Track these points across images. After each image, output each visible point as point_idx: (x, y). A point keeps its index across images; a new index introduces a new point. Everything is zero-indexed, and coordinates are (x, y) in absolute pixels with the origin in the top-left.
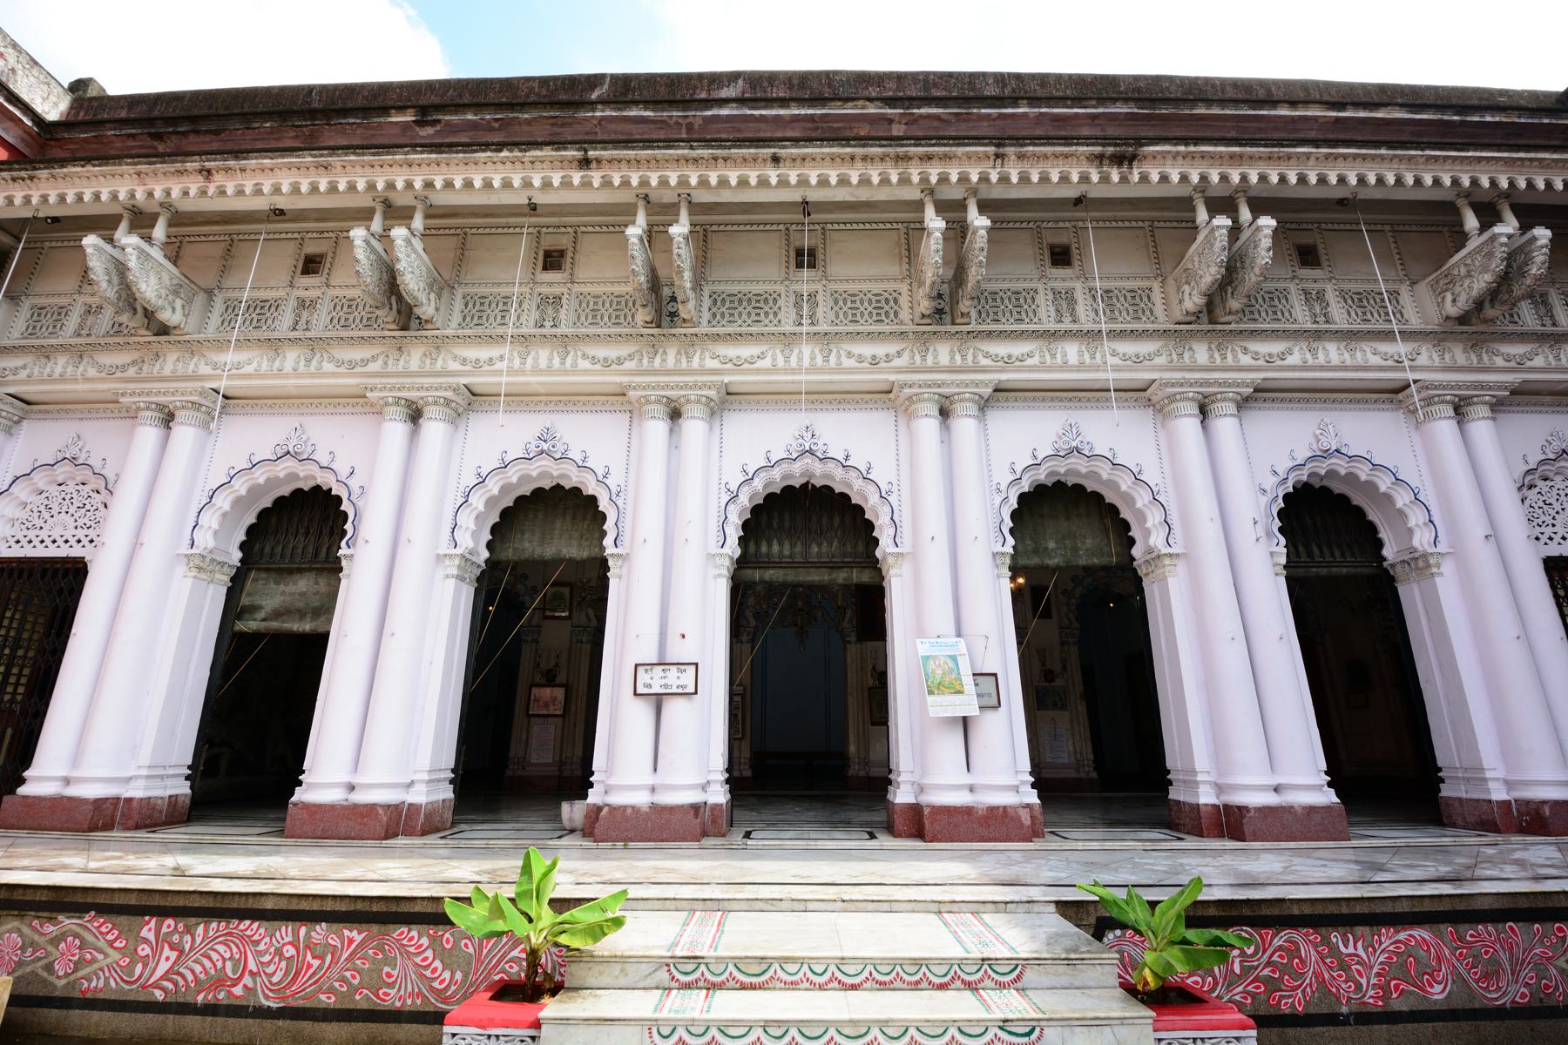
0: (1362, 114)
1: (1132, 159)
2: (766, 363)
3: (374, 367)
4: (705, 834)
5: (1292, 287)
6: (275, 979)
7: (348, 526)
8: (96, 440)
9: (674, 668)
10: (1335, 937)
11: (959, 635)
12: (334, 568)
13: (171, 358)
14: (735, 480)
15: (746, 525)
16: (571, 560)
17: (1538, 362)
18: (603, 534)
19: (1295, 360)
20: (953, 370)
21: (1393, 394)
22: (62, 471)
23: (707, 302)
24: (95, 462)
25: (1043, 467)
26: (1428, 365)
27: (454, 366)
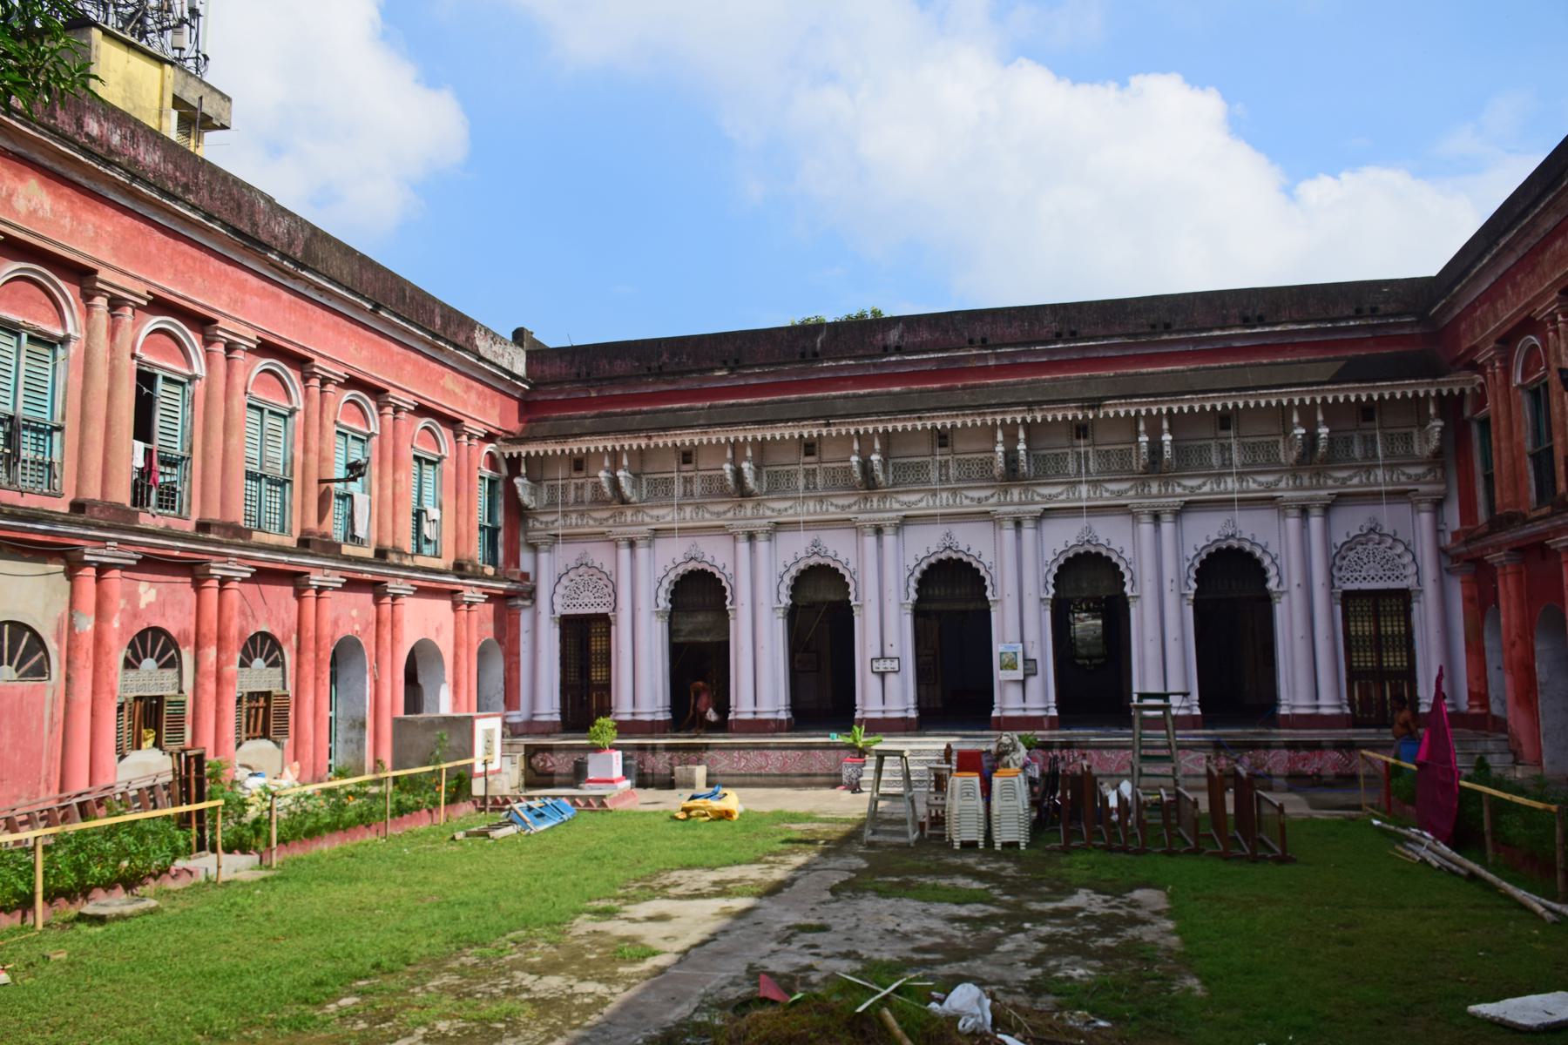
1: (1099, 407)
2: (923, 504)
3: (730, 515)
8: (599, 554)
12: (725, 614)
13: (629, 513)
14: (912, 564)
16: (832, 603)
17: (1356, 481)
19: (1208, 489)
20: (1021, 503)
21: (1270, 502)
22: (582, 570)
24: (597, 564)
26: (1286, 489)
27: (768, 513)
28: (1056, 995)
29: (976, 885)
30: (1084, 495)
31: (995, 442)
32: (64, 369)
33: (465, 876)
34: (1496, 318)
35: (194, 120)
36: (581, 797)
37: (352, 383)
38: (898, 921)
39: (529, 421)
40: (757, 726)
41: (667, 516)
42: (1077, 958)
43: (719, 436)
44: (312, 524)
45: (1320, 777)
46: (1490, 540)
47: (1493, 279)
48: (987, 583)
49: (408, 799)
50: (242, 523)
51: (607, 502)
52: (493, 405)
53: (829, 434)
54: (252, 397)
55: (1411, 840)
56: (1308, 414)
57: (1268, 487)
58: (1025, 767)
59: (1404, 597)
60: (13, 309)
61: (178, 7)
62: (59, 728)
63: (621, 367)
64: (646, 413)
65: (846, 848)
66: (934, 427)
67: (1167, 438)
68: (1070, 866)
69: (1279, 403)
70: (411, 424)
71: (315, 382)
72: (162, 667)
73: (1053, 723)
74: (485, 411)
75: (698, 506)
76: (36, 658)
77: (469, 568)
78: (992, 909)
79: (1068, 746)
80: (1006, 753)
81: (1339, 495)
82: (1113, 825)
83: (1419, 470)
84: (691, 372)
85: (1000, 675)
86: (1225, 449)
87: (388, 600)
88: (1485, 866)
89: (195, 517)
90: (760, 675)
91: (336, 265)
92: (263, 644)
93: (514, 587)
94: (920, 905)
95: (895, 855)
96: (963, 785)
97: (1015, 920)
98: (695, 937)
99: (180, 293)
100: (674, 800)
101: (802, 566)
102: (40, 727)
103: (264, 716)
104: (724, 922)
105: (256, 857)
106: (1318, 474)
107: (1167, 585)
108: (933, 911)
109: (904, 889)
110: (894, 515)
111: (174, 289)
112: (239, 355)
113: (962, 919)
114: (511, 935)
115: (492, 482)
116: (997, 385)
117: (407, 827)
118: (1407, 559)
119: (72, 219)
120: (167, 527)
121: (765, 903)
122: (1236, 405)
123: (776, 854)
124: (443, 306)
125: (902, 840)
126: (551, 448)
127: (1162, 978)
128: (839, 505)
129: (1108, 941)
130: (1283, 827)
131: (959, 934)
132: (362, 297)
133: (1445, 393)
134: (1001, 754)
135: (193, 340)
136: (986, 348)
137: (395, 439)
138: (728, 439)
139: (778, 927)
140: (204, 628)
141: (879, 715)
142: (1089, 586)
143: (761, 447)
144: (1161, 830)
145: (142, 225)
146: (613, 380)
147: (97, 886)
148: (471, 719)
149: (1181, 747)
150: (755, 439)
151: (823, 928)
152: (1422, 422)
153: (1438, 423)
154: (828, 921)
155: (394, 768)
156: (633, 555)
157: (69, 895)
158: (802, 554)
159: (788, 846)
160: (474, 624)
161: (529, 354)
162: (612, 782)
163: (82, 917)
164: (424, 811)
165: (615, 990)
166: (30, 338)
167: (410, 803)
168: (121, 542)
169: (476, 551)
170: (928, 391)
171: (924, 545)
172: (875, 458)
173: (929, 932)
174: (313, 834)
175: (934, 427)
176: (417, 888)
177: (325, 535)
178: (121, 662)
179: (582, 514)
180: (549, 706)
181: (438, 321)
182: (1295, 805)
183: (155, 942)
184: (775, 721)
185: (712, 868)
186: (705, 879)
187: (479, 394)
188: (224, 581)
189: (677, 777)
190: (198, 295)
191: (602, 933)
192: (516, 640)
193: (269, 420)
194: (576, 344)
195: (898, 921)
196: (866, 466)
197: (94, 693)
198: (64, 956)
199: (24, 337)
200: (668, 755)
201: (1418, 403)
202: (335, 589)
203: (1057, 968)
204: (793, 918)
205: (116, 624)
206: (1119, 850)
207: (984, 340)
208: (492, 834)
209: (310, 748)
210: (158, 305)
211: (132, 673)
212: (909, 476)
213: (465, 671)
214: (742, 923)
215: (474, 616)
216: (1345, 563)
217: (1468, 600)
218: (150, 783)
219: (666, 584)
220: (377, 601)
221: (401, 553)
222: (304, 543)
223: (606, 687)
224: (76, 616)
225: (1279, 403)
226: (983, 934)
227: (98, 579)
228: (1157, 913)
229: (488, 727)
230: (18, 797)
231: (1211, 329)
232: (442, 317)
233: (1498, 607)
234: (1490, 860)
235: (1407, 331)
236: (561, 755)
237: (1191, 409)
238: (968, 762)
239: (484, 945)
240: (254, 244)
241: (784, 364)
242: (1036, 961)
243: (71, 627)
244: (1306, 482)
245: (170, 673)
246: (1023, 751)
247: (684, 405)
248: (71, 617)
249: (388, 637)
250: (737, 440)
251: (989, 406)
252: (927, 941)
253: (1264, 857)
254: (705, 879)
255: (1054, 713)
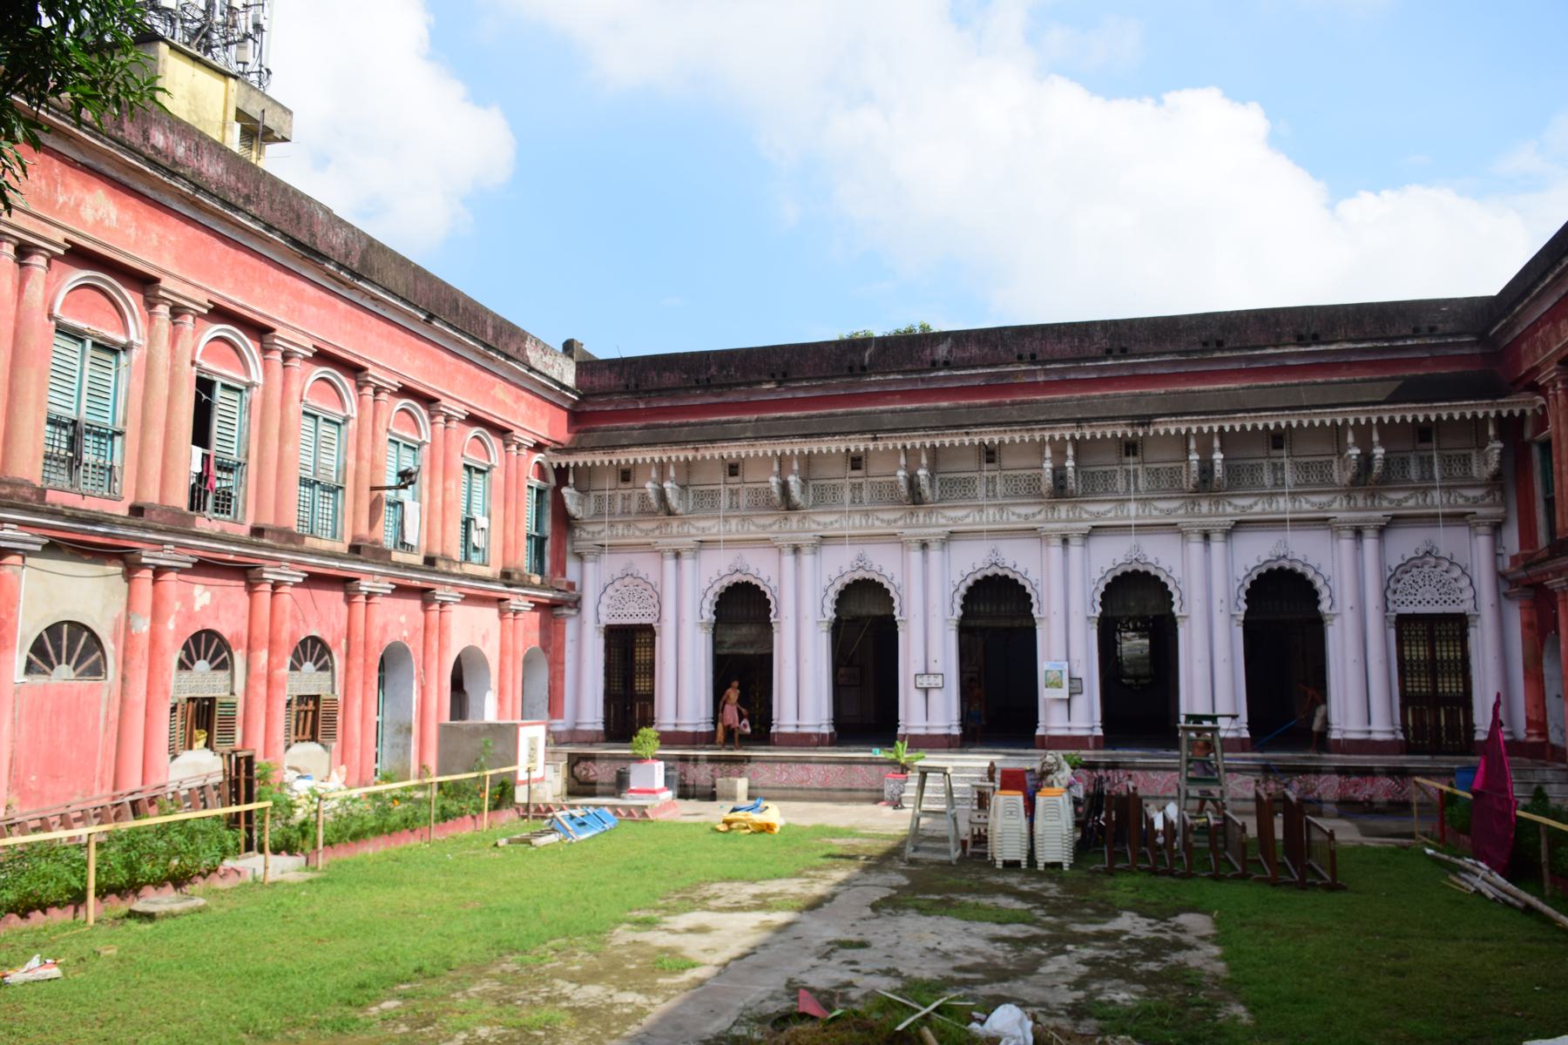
0: (1322, 348)
1: (1149, 424)
2: (970, 520)
3: (776, 528)
4: (950, 746)
5: (1265, 462)
7: (772, 606)
8: (644, 565)
10: (1151, 774)
12: (768, 626)
14: (958, 579)
16: (875, 617)
17: (1411, 503)
19: (1258, 508)
20: (1068, 521)
22: (627, 580)
23: (938, 484)
26: (1339, 509)
27: (814, 526)
28: (1099, 1018)
29: (1019, 905)
30: (1133, 513)
31: (1043, 459)
32: (125, 375)
33: (507, 883)
34: (1559, 338)
35: (256, 133)
36: (623, 807)
37: (405, 391)
38: (938, 939)
39: (578, 432)
40: (801, 740)
41: (712, 528)
42: (1121, 982)
43: (766, 448)
44: (363, 530)
45: (1371, 803)
46: (1550, 565)
47: (1555, 299)
48: (1033, 600)
49: (453, 805)
50: (295, 529)
51: (654, 513)
52: (543, 415)
53: (876, 449)
54: (307, 405)
55: (1466, 871)
56: (1363, 433)
57: (1321, 508)
58: (1069, 787)
59: (1459, 625)
60: (79, 317)
61: (243, 22)
62: (114, 727)
63: (669, 379)
64: (693, 425)
65: (887, 864)
66: (982, 443)
67: (1218, 456)
68: (1113, 888)
69: (1334, 423)
70: (463, 433)
71: (369, 391)
72: (215, 668)
73: (1099, 743)
74: (538, 422)
75: (744, 518)
76: (93, 658)
77: (516, 576)
78: (1034, 930)
79: (1114, 766)
80: (1049, 772)
81: (1395, 517)
82: (1159, 848)
83: (1478, 493)
84: (739, 385)
85: (1045, 694)
86: (1277, 468)
87: (436, 607)
88: (1542, 898)
89: (249, 522)
90: (803, 688)
91: (391, 276)
92: (314, 647)
93: (559, 596)
94: (961, 924)
95: (942, 872)
96: (1008, 803)
97: (1058, 942)
98: (735, 949)
99: (240, 301)
100: (716, 812)
101: (847, 580)
102: (96, 726)
103: (313, 720)
104: (763, 936)
105: (302, 859)
106: (1373, 495)
107: (1217, 606)
108: (974, 930)
109: (945, 907)
110: (940, 530)
111: (235, 299)
112: (295, 363)
113: (1004, 939)
114: (552, 943)
115: (540, 492)
116: (1046, 401)
117: (451, 832)
118: (1464, 582)
119: (137, 228)
120: (223, 531)
121: (806, 917)
122: (1289, 425)
123: (817, 869)
124: (495, 317)
125: (944, 858)
126: (599, 458)
127: (1207, 1005)
128: (887, 519)
129: (1152, 966)
130: (1333, 854)
131: (1000, 954)
132: (416, 307)
133: (1505, 414)
134: (1045, 774)
135: (250, 346)
136: (1038, 363)
137: (446, 447)
138: (774, 453)
139: (818, 942)
140: (256, 632)
141: (922, 732)
142: (1137, 609)
143: (808, 460)
144: (1206, 855)
145: (204, 235)
146: (661, 392)
147: (148, 883)
148: (515, 727)
149: (1229, 770)
150: (801, 452)
151: (863, 945)
152: (1481, 443)
153: (1496, 447)
154: (868, 937)
155: (439, 774)
156: (678, 566)
157: (120, 891)
158: (847, 568)
159: (830, 860)
160: (520, 632)
161: (578, 364)
162: (654, 792)
163: (132, 914)
164: (468, 817)
165: (655, 1001)
166: (95, 344)
167: (454, 809)
168: (177, 545)
169: (523, 559)
170: (976, 406)
171: (970, 561)
172: (922, 473)
173: (970, 952)
174: (358, 836)
175: (982, 443)
176: (460, 894)
177: (375, 542)
178: (175, 663)
179: (628, 525)
180: (592, 715)
181: (490, 331)
182: (1346, 832)
183: (203, 940)
184: (817, 735)
185: (753, 881)
186: (746, 891)
187: (529, 405)
188: (276, 586)
189: (718, 789)
190: (257, 304)
191: (642, 944)
192: (560, 649)
193: (323, 427)
194: (625, 355)
195: (938, 939)
196: (912, 482)
197: (148, 693)
198: (113, 952)
199: (89, 343)
200: (710, 767)
201: (1478, 424)
202: (385, 595)
203: (1100, 991)
204: (833, 934)
205: (171, 625)
206: (1163, 873)
207: (1033, 356)
208: (534, 841)
209: (357, 751)
210: (219, 313)
211: (185, 674)
212: (956, 490)
213: (510, 679)
214: (781, 937)
215: (520, 624)
216: (1400, 586)
217: (1527, 626)
218: (200, 783)
219: (712, 597)
220: (426, 605)
221: (449, 560)
222: (355, 549)
223: (650, 698)
224: (133, 617)
225: (1334, 423)
226: (1025, 955)
227: (155, 582)
228: (1203, 938)
229: (532, 736)
230: (72, 794)
231: (1264, 347)
232: (494, 327)
233: (1558, 633)
234: (1547, 892)
235: (1466, 351)
236: (604, 764)
237: (1243, 427)
238: (1012, 780)
239: (525, 952)
240: (312, 254)
241: (832, 377)
242: (1079, 984)
243: (128, 628)
244: (1360, 503)
245: (223, 675)
246: (1068, 770)
247: (731, 418)
248: (128, 618)
249: (436, 644)
250: (783, 453)
251: (1037, 422)
252: (968, 961)
253: (1313, 885)
254: (746, 891)
255: (1099, 732)
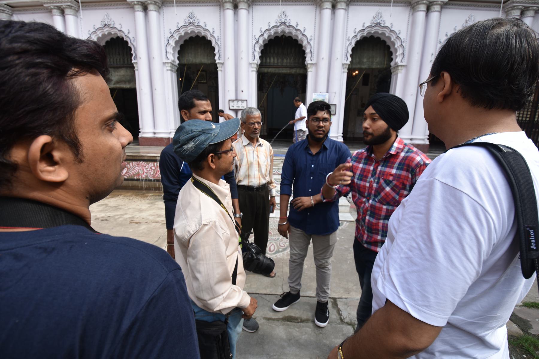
6: (152, 173)
7: (132, 52)
9: (240, 101)
11: (327, 92)
12: (132, 67)
15: (262, 52)
16: (205, 64)
18: (215, 55)
25: (366, 31)
158: (182, 24)
